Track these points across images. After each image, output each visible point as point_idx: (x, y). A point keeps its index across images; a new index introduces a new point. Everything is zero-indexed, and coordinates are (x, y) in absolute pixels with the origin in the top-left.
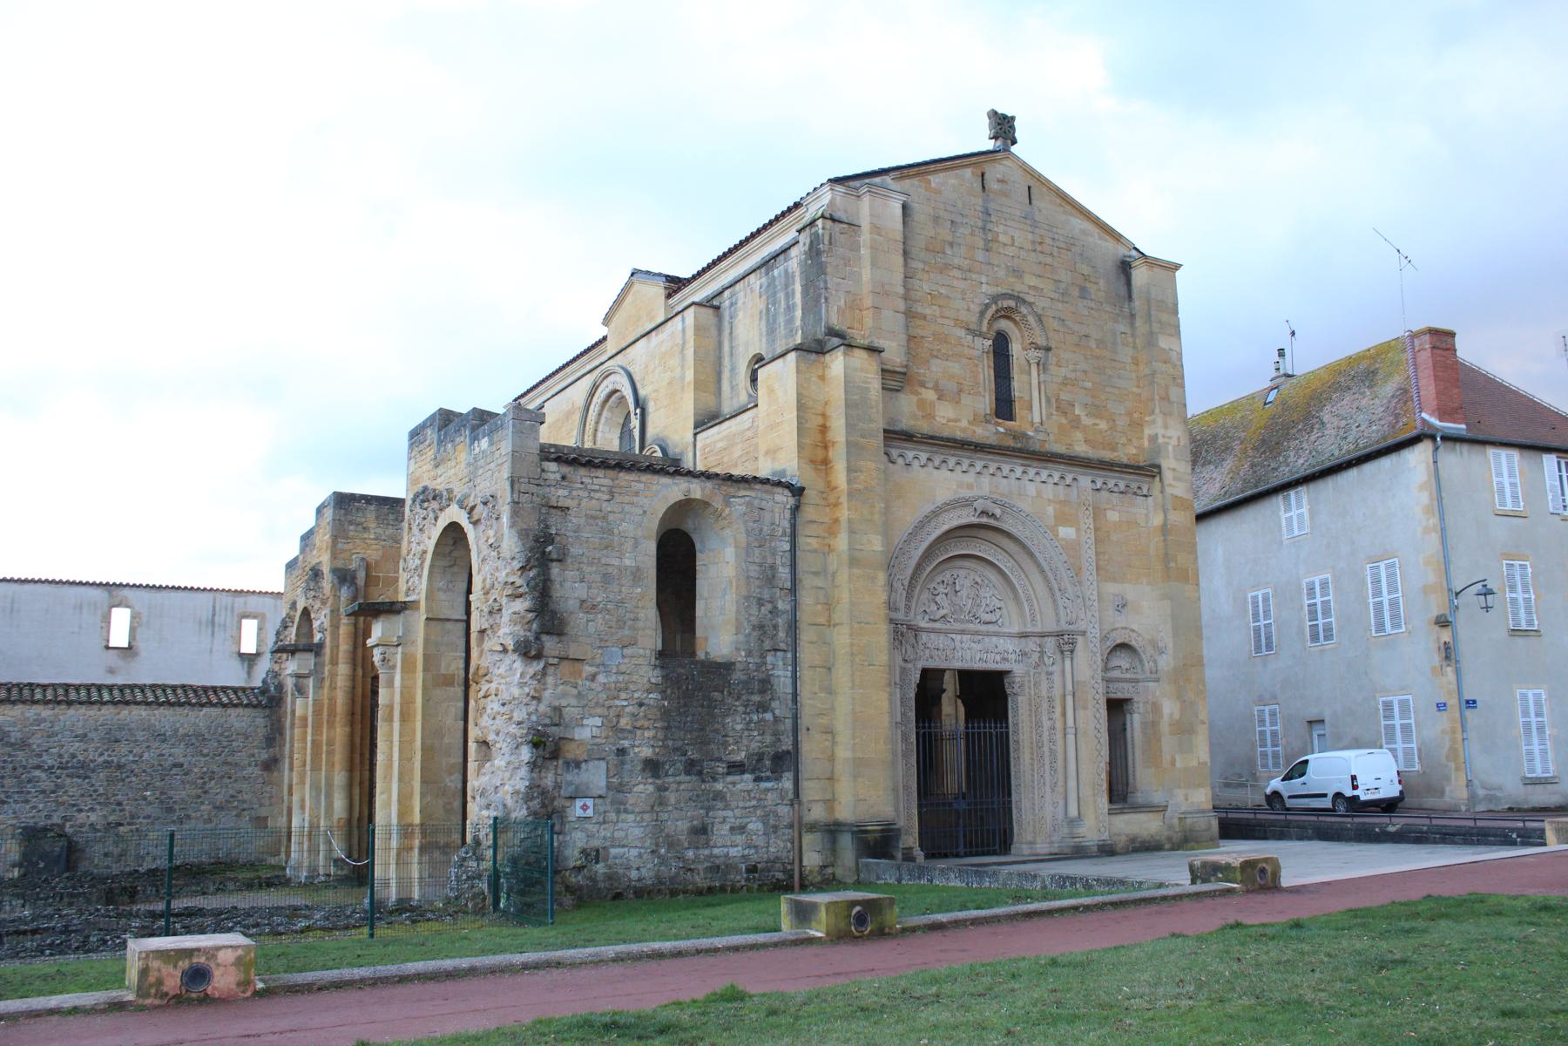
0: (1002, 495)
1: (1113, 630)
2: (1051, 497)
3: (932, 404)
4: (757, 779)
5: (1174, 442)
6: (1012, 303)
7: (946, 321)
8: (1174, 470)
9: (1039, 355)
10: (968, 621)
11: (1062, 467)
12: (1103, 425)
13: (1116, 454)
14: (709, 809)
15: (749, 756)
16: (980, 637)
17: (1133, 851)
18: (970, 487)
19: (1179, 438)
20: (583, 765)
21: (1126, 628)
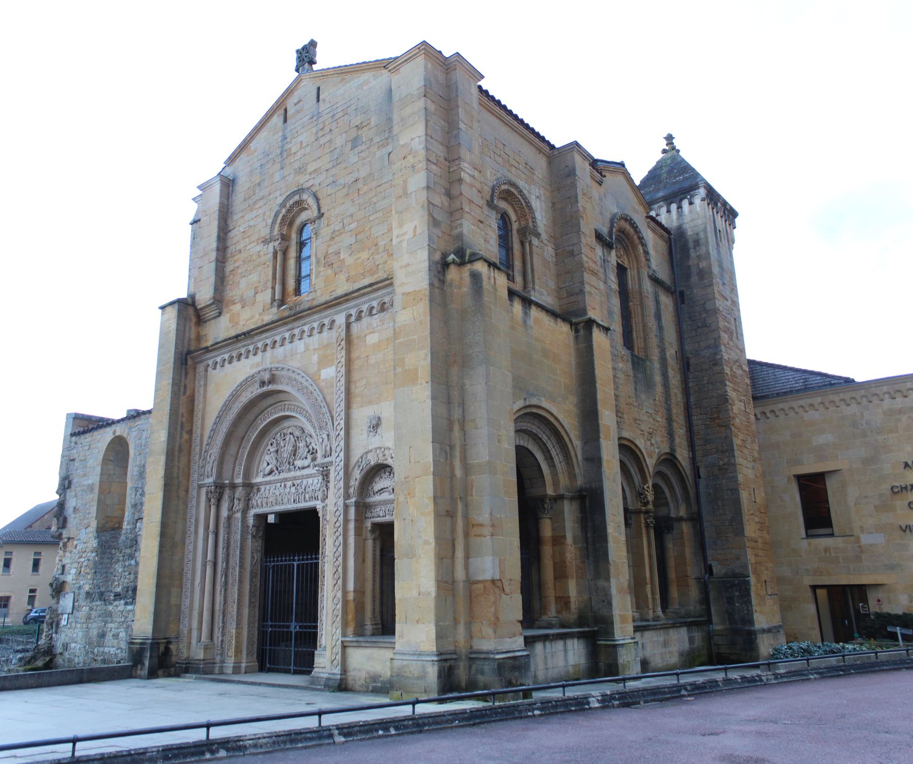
0: (278, 362)
1: (366, 453)
2: (316, 347)
3: (238, 314)
4: (126, 604)
5: (410, 234)
6: (296, 198)
7: (252, 245)
8: (408, 265)
9: (315, 226)
10: (289, 470)
11: (316, 316)
12: (364, 255)
13: (376, 276)
14: (106, 622)
15: (123, 589)
16: (299, 481)
17: (372, 691)
18: (258, 365)
19: (416, 227)
20: (66, 596)
21: (380, 448)
